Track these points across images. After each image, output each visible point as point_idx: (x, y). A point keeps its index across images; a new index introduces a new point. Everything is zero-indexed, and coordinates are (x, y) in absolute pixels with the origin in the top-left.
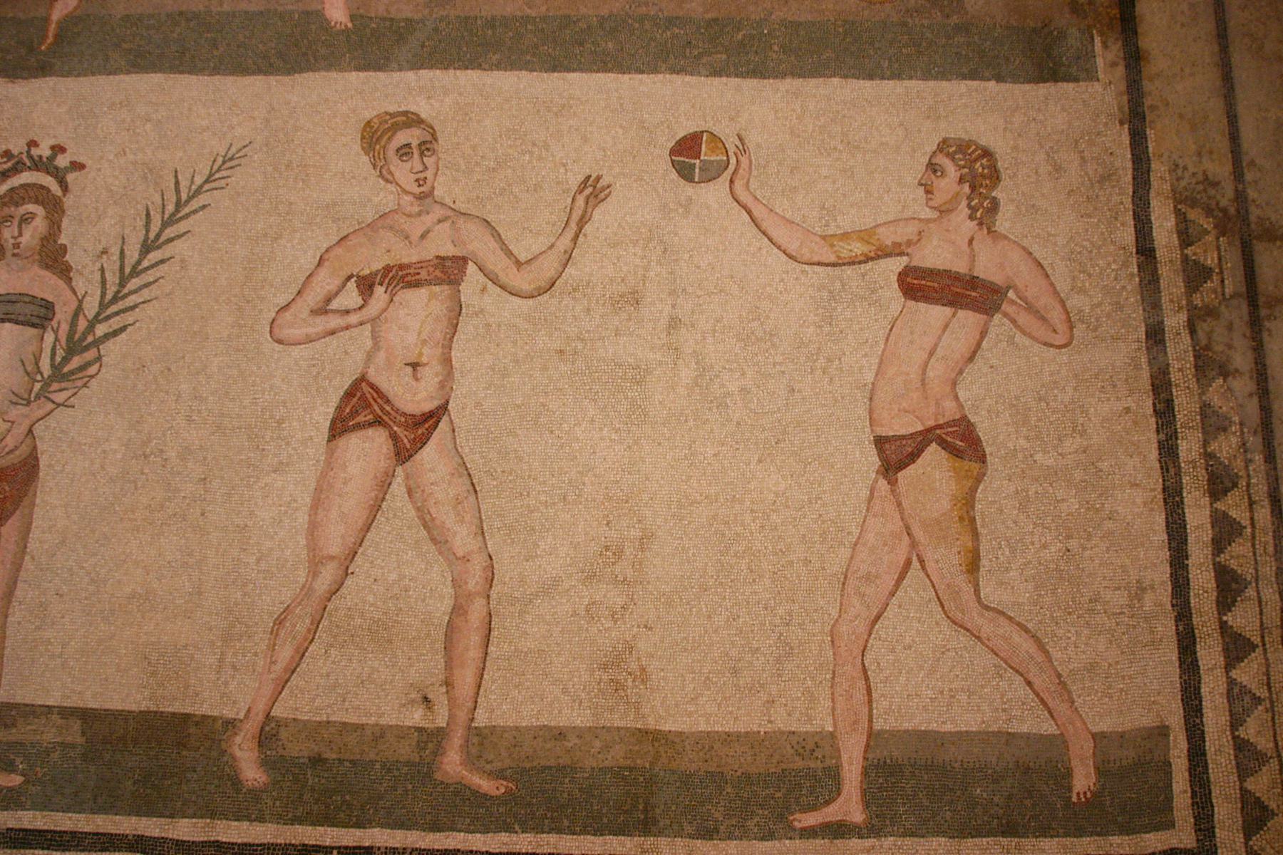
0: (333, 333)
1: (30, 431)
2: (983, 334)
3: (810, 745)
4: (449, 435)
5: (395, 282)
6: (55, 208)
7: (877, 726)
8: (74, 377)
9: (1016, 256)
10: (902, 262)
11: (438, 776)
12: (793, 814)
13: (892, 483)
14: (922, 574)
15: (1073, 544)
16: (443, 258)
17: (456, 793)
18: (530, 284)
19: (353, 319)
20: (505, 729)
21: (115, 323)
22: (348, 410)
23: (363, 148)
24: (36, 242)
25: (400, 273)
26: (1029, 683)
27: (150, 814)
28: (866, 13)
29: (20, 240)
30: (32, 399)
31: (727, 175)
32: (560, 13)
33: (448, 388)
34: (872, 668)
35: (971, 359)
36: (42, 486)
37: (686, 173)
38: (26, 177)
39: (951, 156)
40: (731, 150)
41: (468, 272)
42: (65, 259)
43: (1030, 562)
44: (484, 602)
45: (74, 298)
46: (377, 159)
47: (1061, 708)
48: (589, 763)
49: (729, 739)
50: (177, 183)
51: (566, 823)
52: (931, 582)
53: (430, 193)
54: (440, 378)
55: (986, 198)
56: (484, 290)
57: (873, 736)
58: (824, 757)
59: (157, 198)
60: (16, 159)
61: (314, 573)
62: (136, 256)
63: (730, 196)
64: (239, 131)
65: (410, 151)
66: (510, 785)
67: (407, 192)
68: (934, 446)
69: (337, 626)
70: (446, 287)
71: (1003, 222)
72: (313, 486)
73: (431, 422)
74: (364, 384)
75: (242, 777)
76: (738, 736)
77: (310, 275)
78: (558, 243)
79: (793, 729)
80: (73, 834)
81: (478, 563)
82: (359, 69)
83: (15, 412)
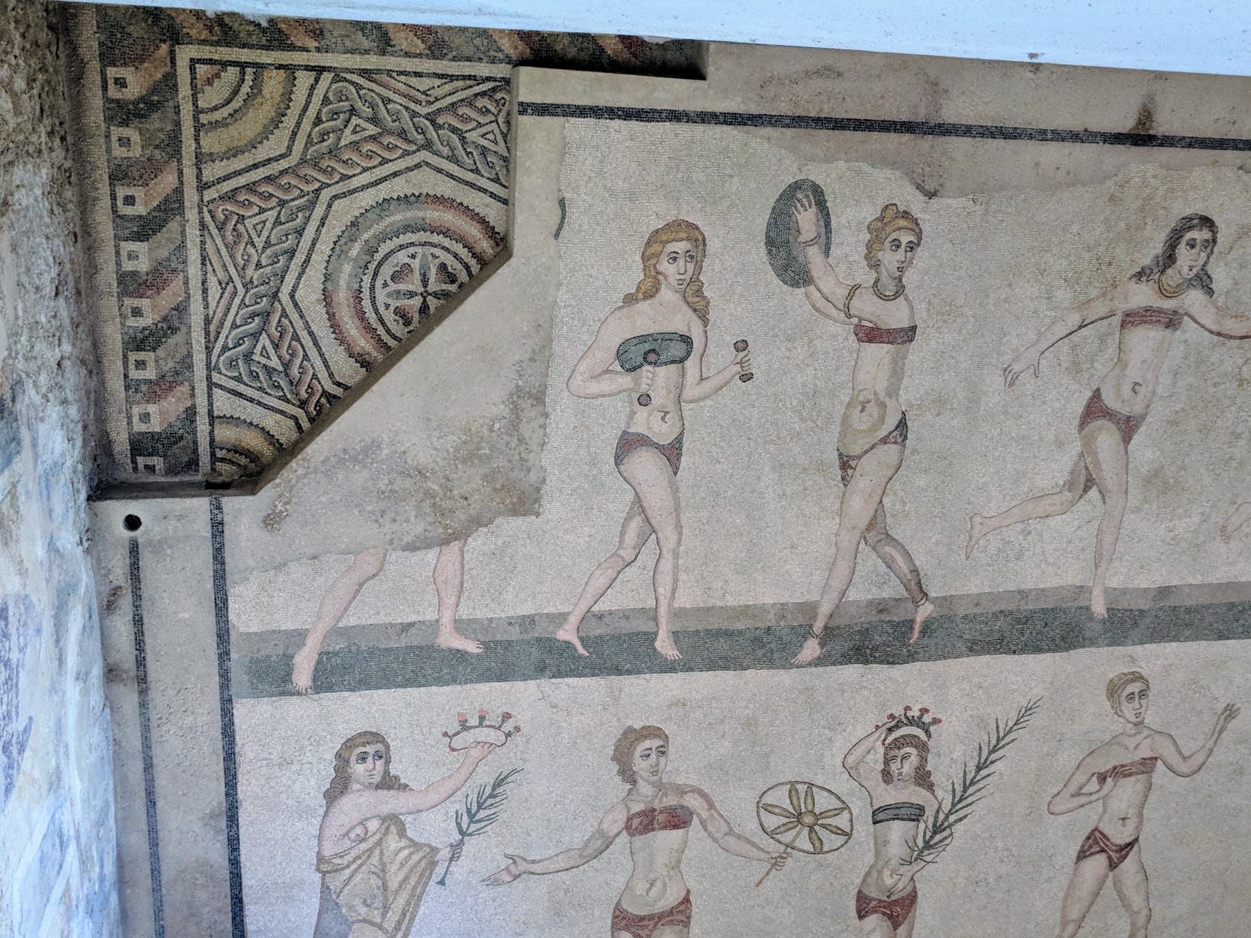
0: (1083, 806)
6: (923, 748)
16: (1145, 759)
19: (1094, 797)
21: (961, 814)
38: (904, 731)
44: (1143, 931)
50: (998, 727)
53: (1142, 723)
59: (986, 738)
62: (973, 774)
64: (1035, 691)
67: (1129, 722)
72: (1066, 887)
77: (1072, 775)
81: (1145, 912)
82: (1108, 645)
83: (903, 870)
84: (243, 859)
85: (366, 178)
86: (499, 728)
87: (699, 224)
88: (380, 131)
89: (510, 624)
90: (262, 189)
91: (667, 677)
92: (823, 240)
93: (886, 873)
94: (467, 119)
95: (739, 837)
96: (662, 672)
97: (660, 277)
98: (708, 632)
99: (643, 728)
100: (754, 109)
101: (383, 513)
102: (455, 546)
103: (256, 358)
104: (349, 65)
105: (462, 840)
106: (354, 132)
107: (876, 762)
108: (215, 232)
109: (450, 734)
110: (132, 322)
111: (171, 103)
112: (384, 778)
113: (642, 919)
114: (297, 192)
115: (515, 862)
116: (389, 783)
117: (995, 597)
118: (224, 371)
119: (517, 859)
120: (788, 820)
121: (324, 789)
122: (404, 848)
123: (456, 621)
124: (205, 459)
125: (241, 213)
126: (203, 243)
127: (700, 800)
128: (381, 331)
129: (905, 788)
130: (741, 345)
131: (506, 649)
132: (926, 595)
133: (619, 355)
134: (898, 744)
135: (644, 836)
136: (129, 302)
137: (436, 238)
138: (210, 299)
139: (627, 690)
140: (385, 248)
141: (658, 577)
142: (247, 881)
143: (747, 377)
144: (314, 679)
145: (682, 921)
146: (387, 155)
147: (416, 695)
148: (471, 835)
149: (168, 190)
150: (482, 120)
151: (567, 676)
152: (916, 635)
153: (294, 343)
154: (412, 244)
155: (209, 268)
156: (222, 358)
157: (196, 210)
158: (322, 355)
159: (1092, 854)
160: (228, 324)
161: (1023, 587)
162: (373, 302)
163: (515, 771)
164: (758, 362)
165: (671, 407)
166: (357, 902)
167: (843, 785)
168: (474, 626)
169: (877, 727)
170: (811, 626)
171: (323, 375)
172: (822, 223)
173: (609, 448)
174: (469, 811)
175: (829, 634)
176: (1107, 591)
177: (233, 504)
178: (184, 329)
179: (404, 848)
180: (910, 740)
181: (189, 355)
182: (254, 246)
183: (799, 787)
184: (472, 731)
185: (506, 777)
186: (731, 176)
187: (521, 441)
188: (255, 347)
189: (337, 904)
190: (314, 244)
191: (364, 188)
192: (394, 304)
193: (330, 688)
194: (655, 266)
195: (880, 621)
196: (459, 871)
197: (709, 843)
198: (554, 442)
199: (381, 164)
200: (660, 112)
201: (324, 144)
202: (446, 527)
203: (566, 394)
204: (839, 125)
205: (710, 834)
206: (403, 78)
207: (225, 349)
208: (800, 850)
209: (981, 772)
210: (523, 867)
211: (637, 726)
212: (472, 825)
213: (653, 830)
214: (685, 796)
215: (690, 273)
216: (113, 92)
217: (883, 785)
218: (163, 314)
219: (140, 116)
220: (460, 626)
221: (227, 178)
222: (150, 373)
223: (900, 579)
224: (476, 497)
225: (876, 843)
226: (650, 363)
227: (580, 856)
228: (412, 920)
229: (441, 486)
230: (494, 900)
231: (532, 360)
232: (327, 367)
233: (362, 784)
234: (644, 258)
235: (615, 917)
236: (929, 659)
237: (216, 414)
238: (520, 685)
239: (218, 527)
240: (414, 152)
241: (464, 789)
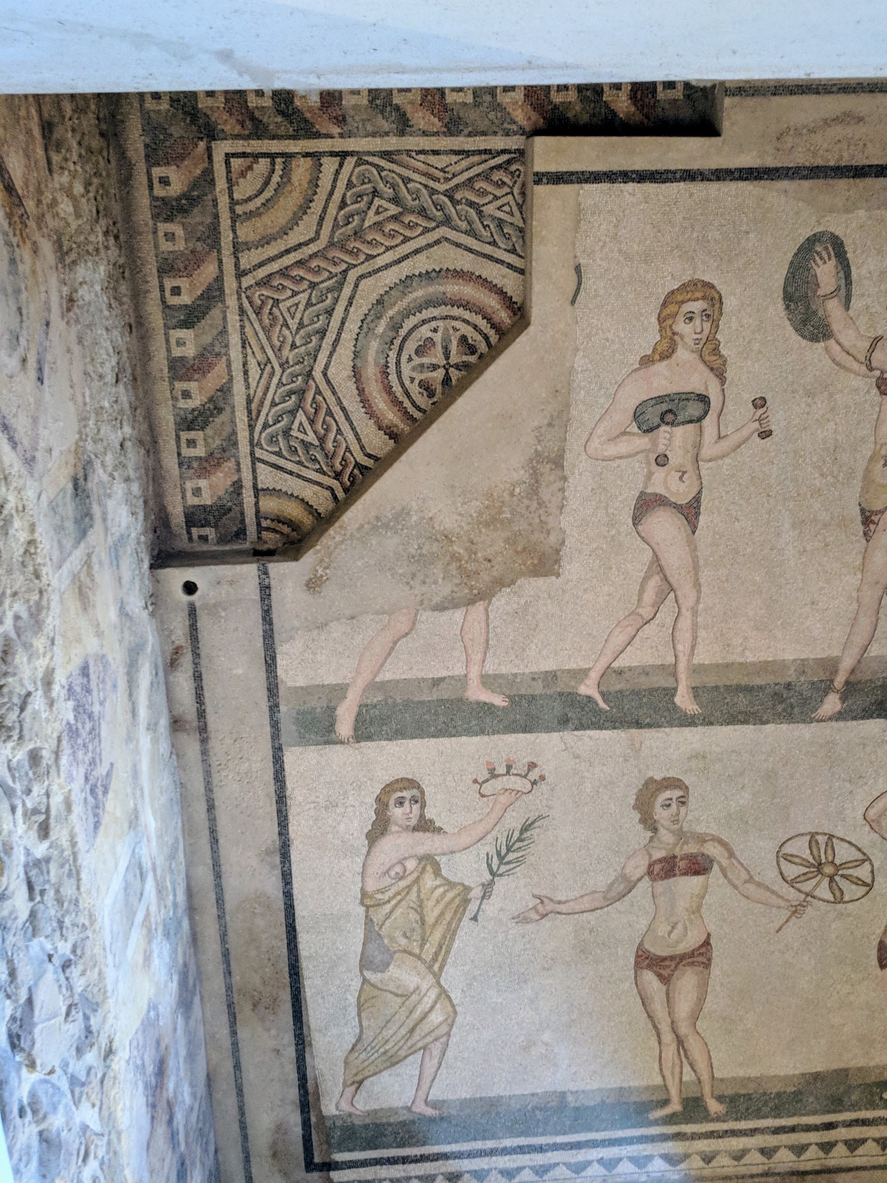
84: (295, 892)
85: (389, 257)
86: (525, 777)
87: (715, 282)
88: (401, 210)
89: (534, 679)
90: (294, 273)
92: (843, 292)
94: (483, 193)
95: (759, 885)
97: (676, 338)
98: (727, 688)
99: (664, 779)
100: (770, 162)
101: (414, 575)
102: (480, 606)
103: (294, 433)
104: (371, 148)
105: (493, 880)
106: (377, 213)
108: (253, 316)
109: (480, 781)
110: (182, 404)
111: (210, 197)
112: (420, 821)
113: (664, 959)
114: (326, 274)
115: (542, 902)
116: (424, 826)
118: (265, 447)
119: (545, 900)
120: (807, 870)
121: (366, 831)
122: (440, 886)
123: (482, 676)
124: (251, 530)
125: (276, 297)
126: (242, 327)
127: (720, 848)
128: (407, 404)
130: (759, 402)
131: (530, 703)
133: (636, 416)
135: (666, 881)
136: (180, 386)
137: (456, 312)
138: (250, 380)
139: (647, 743)
140: (408, 324)
141: (677, 634)
142: (300, 911)
143: (765, 434)
144: (356, 729)
146: (408, 233)
147: (448, 746)
148: (501, 875)
149: (210, 279)
150: (499, 193)
151: (589, 728)
153: (328, 418)
154: (434, 318)
155: (249, 351)
156: (264, 435)
157: (236, 296)
158: (353, 429)
160: (267, 403)
162: (399, 377)
163: (540, 818)
164: (777, 420)
165: (689, 467)
166: (398, 934)
167: (865, 837)
168: (500, 681)
170: (832, 681)
171: (355, 447)
172: (842, 274)
173: (627, 509)
174: (499, 853)
175: (851, 688)
177: (278, 569)
178: (228, 409)
179: (440, 886)
181: (234, 433)
182: (288, 328)
183: (822, 839)
185: (533, 823)
186: (748, 233)
187: (541, 504)
188: (293, 422)
189: (379, 935)
190: (343, 324)
191: (387, 267)
192: (418, 377)
193: (369, 738)
194: (671, 326)
196: (491, 908)
197: (729, 890)
198: (573, 503)
199: (403, 242)
200: (675, 172)
201: (350, 226)
202: (471, 588)
203: (584, 457)
204: (859, 172)
205: (730, 881)
206: (421, 157)
207: (266, 426)
208: (820, 899)
210: (550, 907)
211: (658, 777)
213: (675, 875)
215: (706, 332)
216: (159, 191)
218: (208, 395)
219: (183, 211)
221: (261, 265)
222: (200, 451)
224: (499, 559)
226: (667, 424)
227: (604, 898)
228: (448, 952)
229: (466, 549)
230: (523, 937)
231: (550, 425)
232: (359, 440)
233: (400, 826)
234: (661, 320)
235: (638, 956)
237: (260, 486)
238: (544, 737)
239: (265, 590)
240: (434, 229)
241: (494, 833)
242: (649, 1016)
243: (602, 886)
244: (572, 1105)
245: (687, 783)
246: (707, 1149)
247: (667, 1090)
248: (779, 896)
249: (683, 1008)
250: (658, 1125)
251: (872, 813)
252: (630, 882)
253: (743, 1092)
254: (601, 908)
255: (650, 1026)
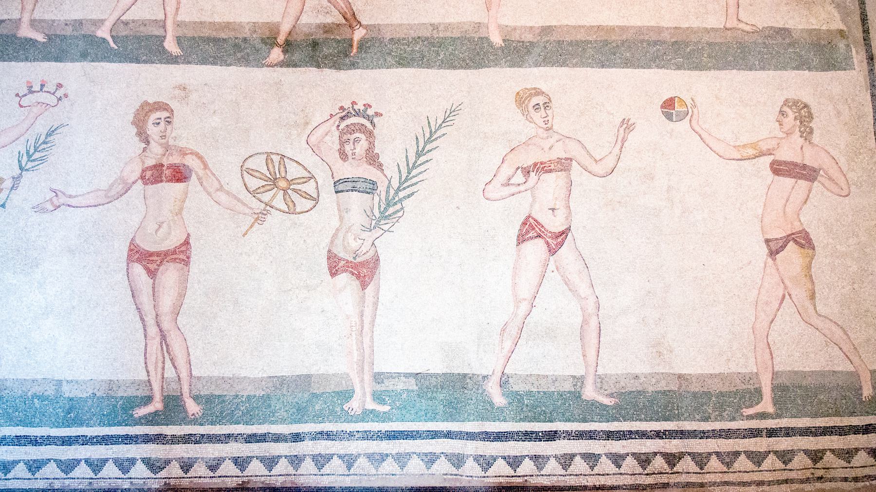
1: (373, 244)
2: (810, 191)
3: (747, 379)
4: (573, 242)
5: (540, 170)
6: (370, 134)
7: (776, 370)
8: (391, 218)
9: (823, 154)
10: (772, 158)
11: (584, 397)
12: (742, 409)
13: (774, 260)
14: (790, 301)
15: (856, 286)
17: (593, 405)
18: (602, 171)
19: (522, 188)
20: (611, 375)
22: (524, 231)
23: (517, 106)
24: (363, 153)
25: (541, 166)
26: (841, 349)
27: (453, 420)
28: (746, 38)
29: (354, 151)
30: (372, 228)
31: (688, 118)
32: (603, 39)
33: (569, 220)
34: (771, 343)
35: (805, 202)
36: (383, 270)
37: (669, 117)
39: (790, 107)
40: (689, 106)
41: (573, 165)
42: (379, 160)
43: (837, 295)
44: (596, 318)
45: (387, 179)
46: (524, 110)
47: (855, 359)
48: (651, 389)
49: (711, 377)
50: (429, 122)
51: (643, 416)
52: (795, 304)
54: (566, 215)
55: (808, 127)
56: (581, 173)
57: (775, 375)
58: (754, 384)
60: (347, 111)
61: (518, 307)
63: (690, 128)
65: (539, 107)
66: (616, 400)
67: (540, 127)
68: (791, 242)
69: (531, 331)
70: (563, 172)
71: (816, 138)
73: (563, 236)
74: (530, 219)
75: (494, 402)
76: (716, 375)
78: (613, 151)
79: (739, 372)
80: (418, 432)
81: (592, 299)
83: (365, 235)
86: (53, 94)
89: (66, 24)
91: (172, 67)
93: (350, 238)
95: (228, 193)
96: (169, 63)
99: (155, 103)
107: (333, 143)
109: (20, 95)
113: (151, 254)
117: (410, 27)
119: (59, 193)
120: (266, 183)
123: (31, 20)
127: (198, 161)
129: (358, 166)
132: (359, 22)
134: (350, 129)
135: (154, 186)
145: (183, 260)
148: (27, 170)
152: (355, 50)
159: (531, 238)
161: (433, 21)
163: (62, 126)
167: (309, 159)
168: (43, 24)
169: (331, 116)
170: (275, 38)
174: (28, 152)
176: (499, 26)
180: (362, 128)
183: (274, 157)
184: (35, 94)
195: (327, 39)
197: (204, 195)
205: (205, 189)
208: (277, 209)
209: (420, 159)
210: (62, 200)
211: (151, 101)
212: (29, 163)
213: (162, 181)
214: (186, 157)
217: (340, 161)
220: (33, 23)
223: (339, 11)
225: (339, 210)
227: (106, 196)
230: (39, 225)
235: (131, 250)
236: (367, 68)
238: (69, 65)
241: (26, 136)
242: (138, 308)
243: (104, 185)
244: (67, 395)
245: (173, 107)
246: (186, 455)
247: (151, 386)
248: (244, 204)
249: (167, 302)
250: (142, 424)
251: (313, 139)
252: (127, 184)
253: (217, 393)
254: (103, 205)
255: (138, 318)
